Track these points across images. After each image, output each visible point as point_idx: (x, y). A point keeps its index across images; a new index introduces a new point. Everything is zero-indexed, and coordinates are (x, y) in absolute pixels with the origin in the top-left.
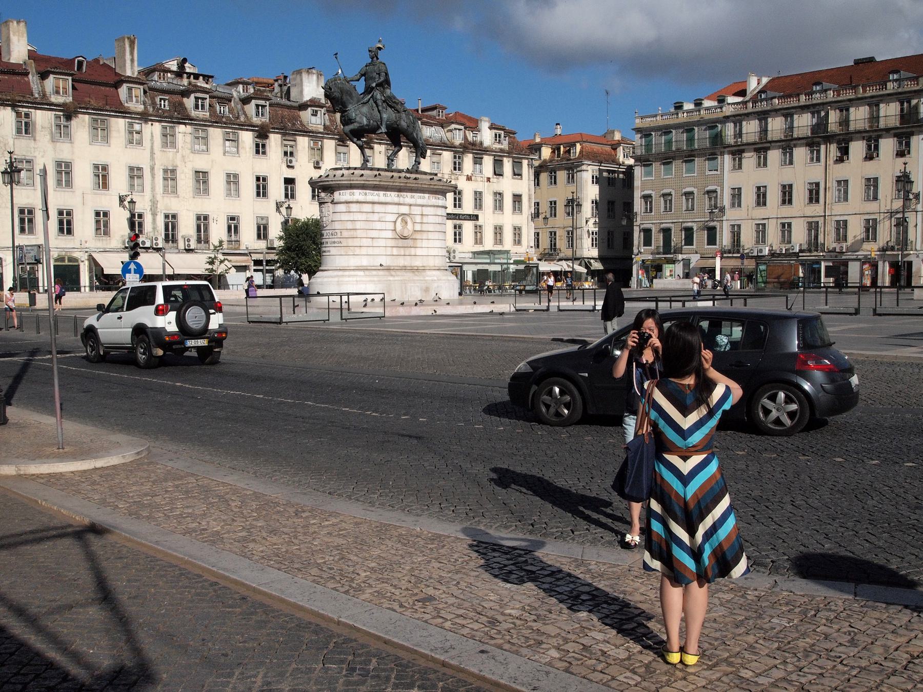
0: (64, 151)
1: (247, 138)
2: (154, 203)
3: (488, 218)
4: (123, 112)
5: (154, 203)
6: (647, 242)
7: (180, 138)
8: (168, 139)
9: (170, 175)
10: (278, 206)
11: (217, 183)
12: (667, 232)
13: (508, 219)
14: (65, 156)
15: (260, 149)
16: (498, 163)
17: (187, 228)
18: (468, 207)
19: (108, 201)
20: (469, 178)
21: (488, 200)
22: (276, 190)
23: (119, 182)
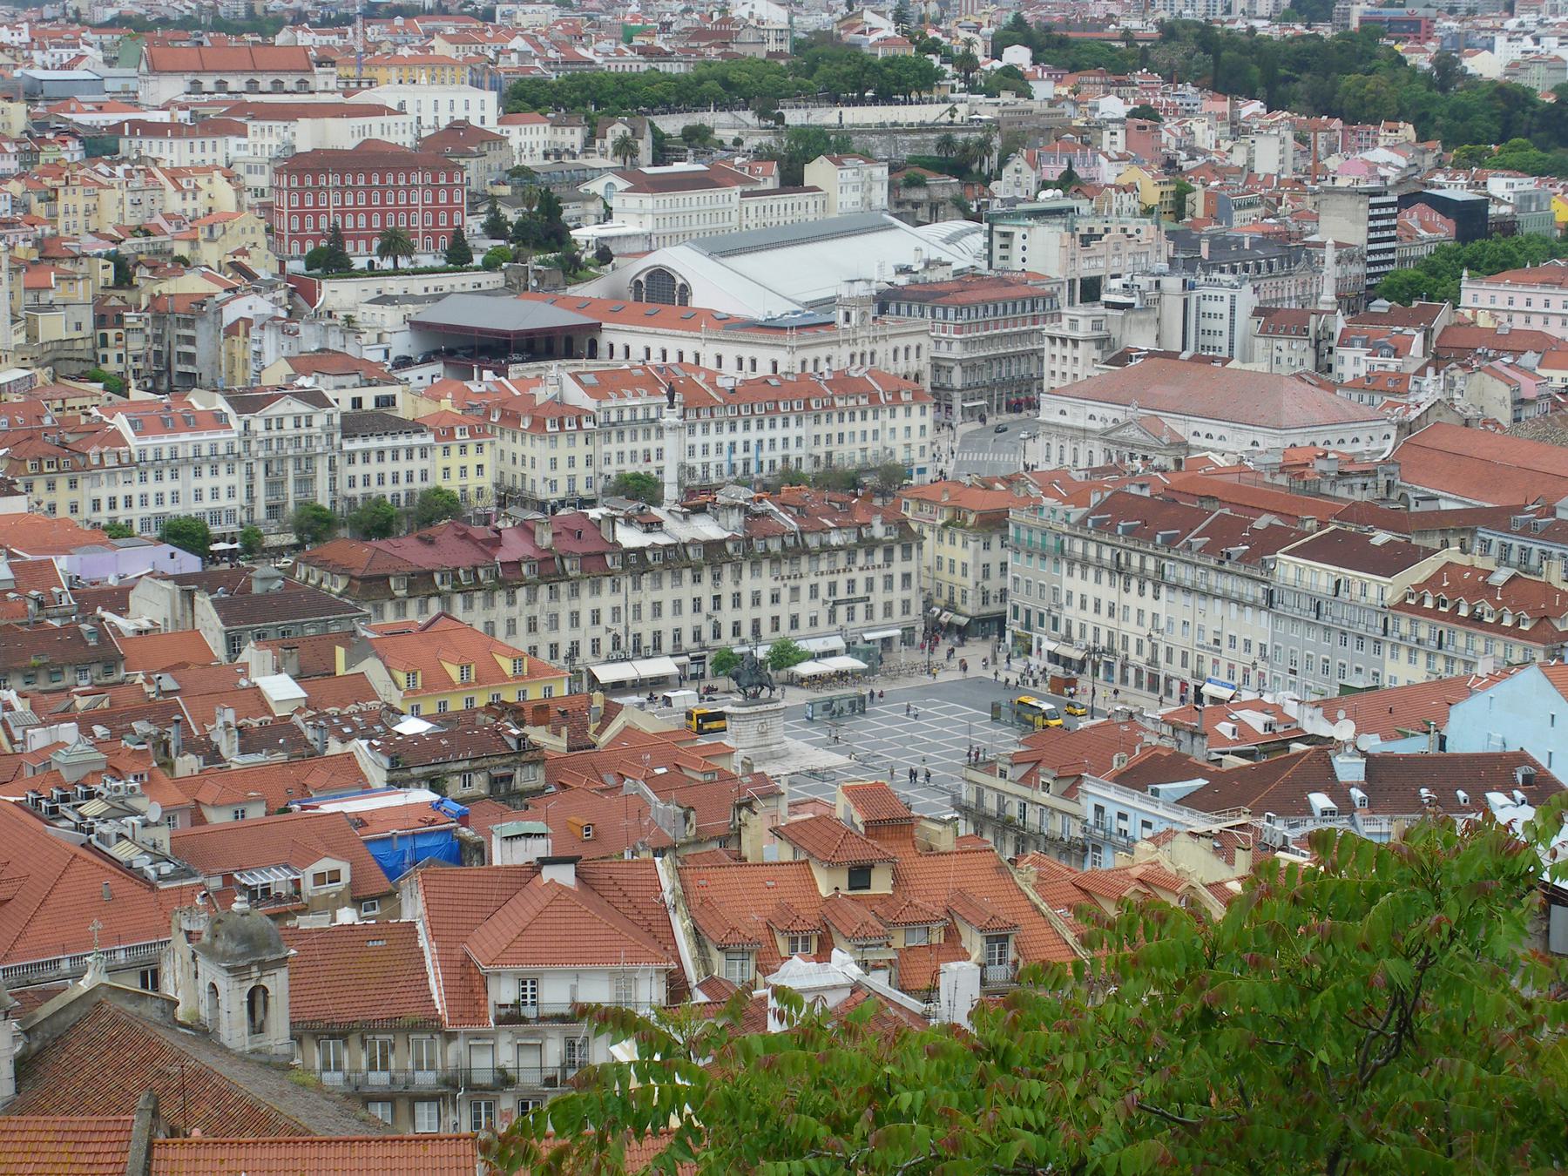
0: (575, 605)
1: (687, 574)
2: (627, 628)
3: (878, 598)
4: (610, 574)
5: (627, 628)
6: (1016, 617)
7: (644, 582)
8: (637, 586)
9: (638, 608)
10: (709, 617)
11: (667, 608)
12: (1028, 612)
13: (897, 595)
14: (576, 608)
15: (697, 579)
16: (889, 552)
17: (647, 641)
18: (860, 591)
19: (599, 632)
20: (861, 569)
21: (879, 583)
22: (707, 605)
23: (606, 617)
